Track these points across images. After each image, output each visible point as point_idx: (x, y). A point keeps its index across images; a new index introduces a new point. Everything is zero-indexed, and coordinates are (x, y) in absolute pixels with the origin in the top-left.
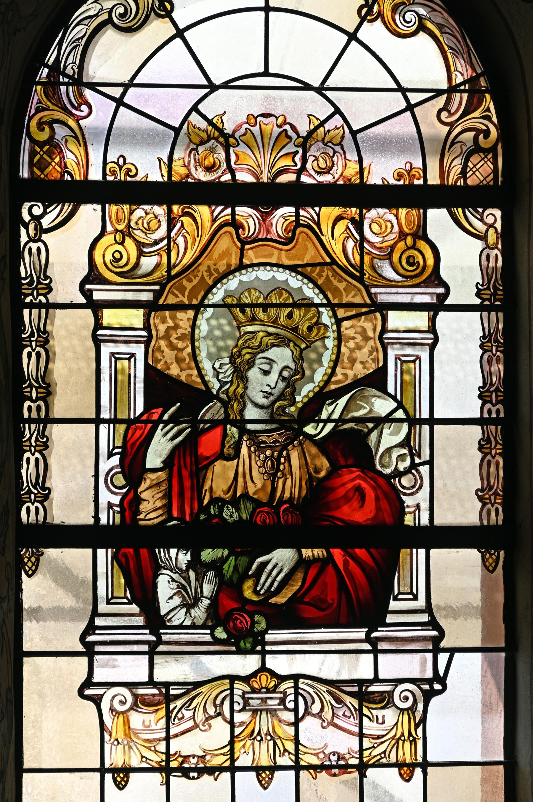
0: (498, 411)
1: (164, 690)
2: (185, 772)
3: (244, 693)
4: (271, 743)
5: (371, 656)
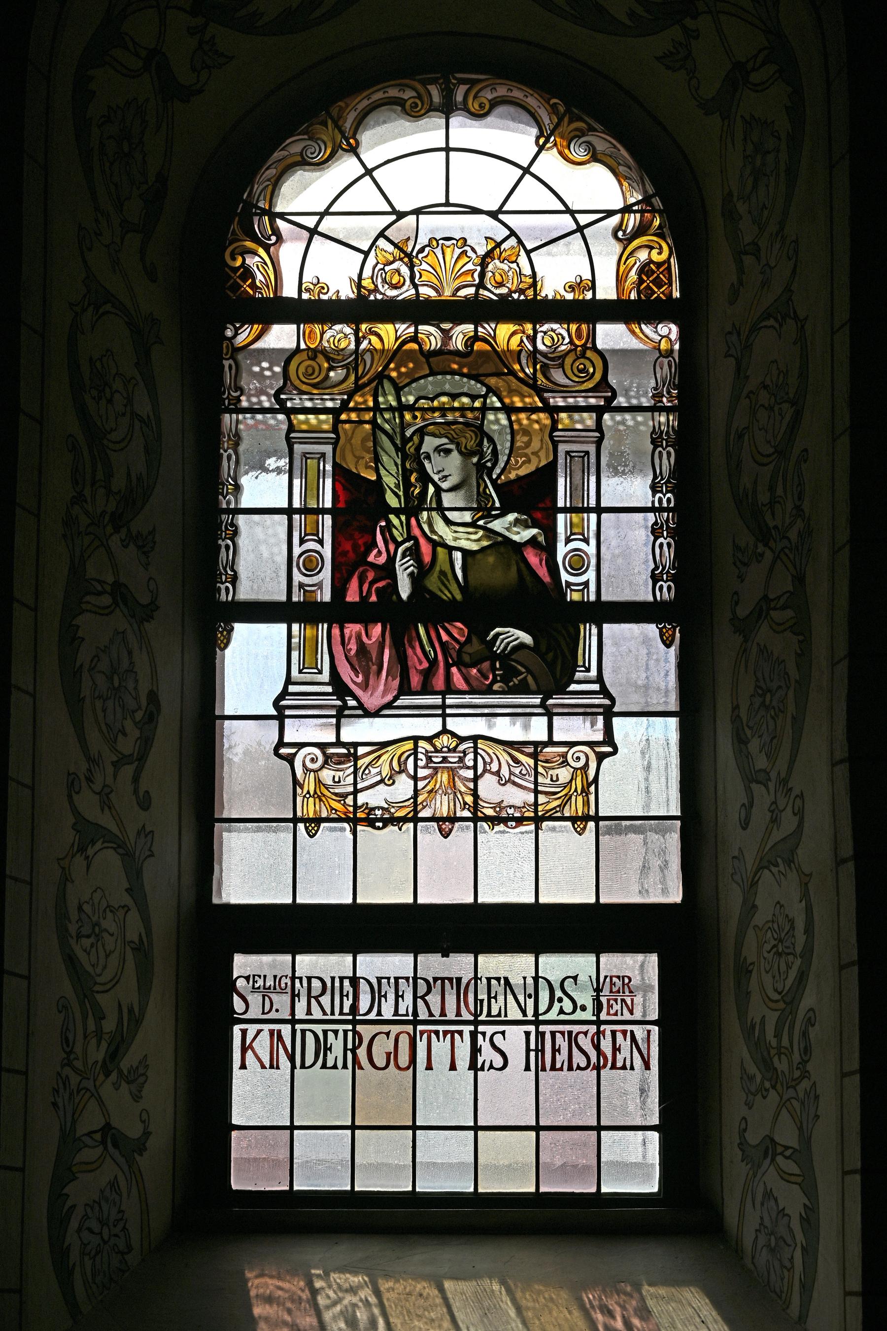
0: (669, 500)
1: (352, 751)
2: (371, 823)
4: (451, 796)
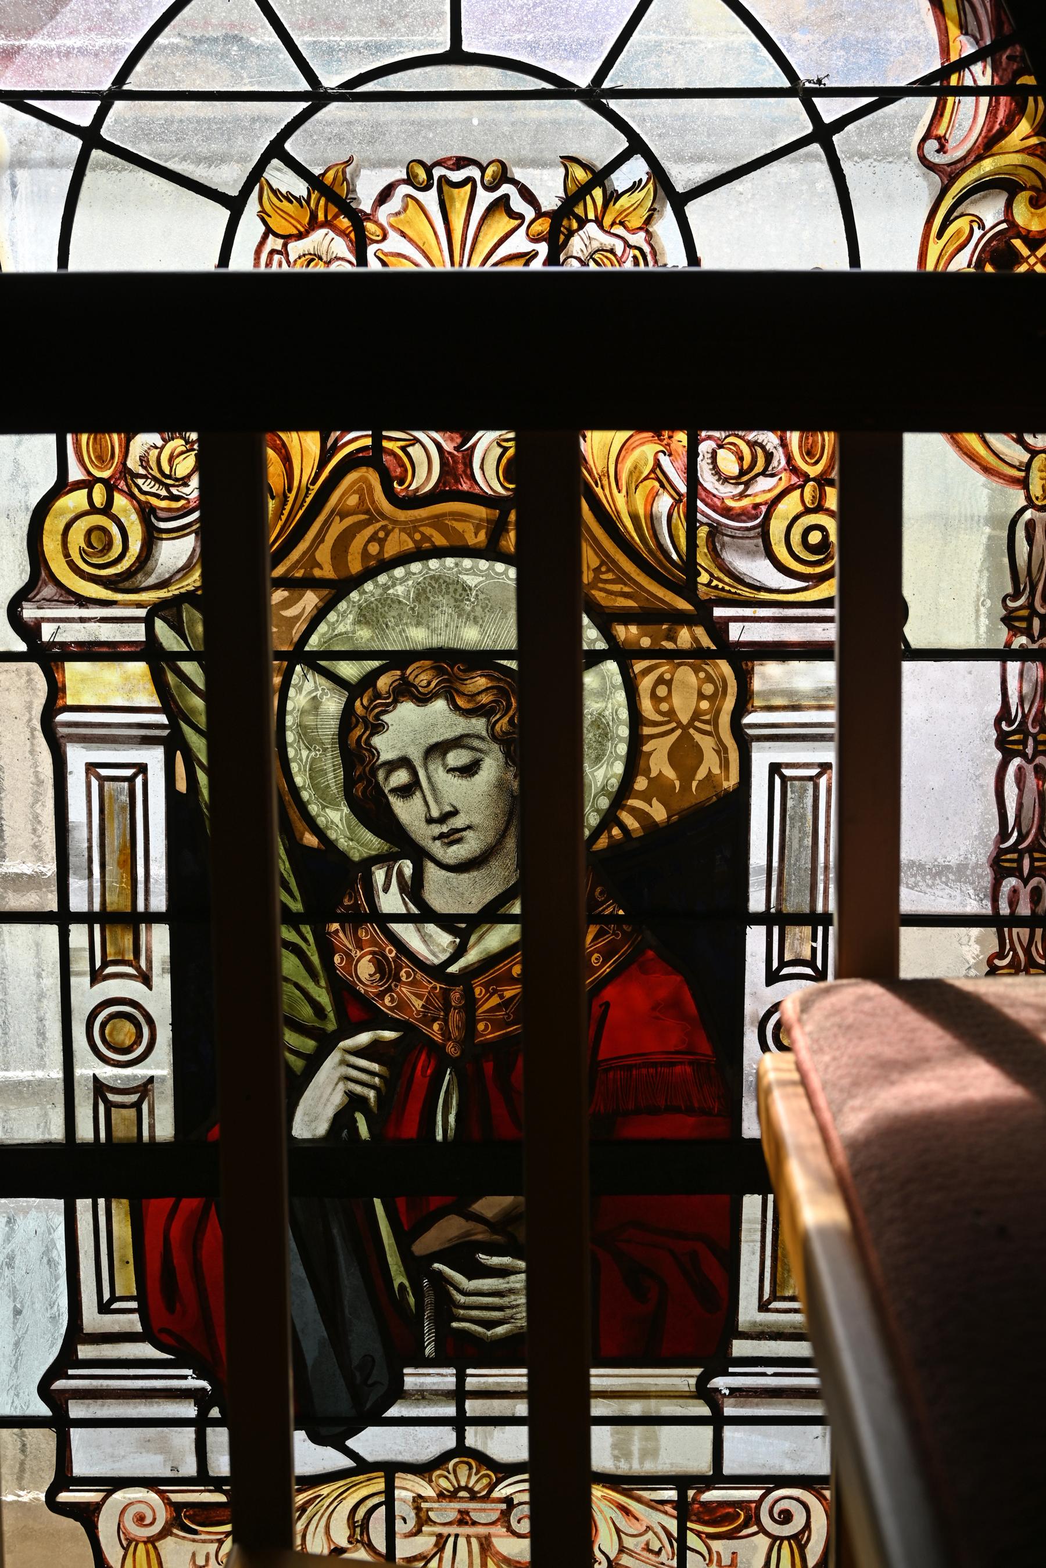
3: (419, 1498)
5: (707, 1432)
